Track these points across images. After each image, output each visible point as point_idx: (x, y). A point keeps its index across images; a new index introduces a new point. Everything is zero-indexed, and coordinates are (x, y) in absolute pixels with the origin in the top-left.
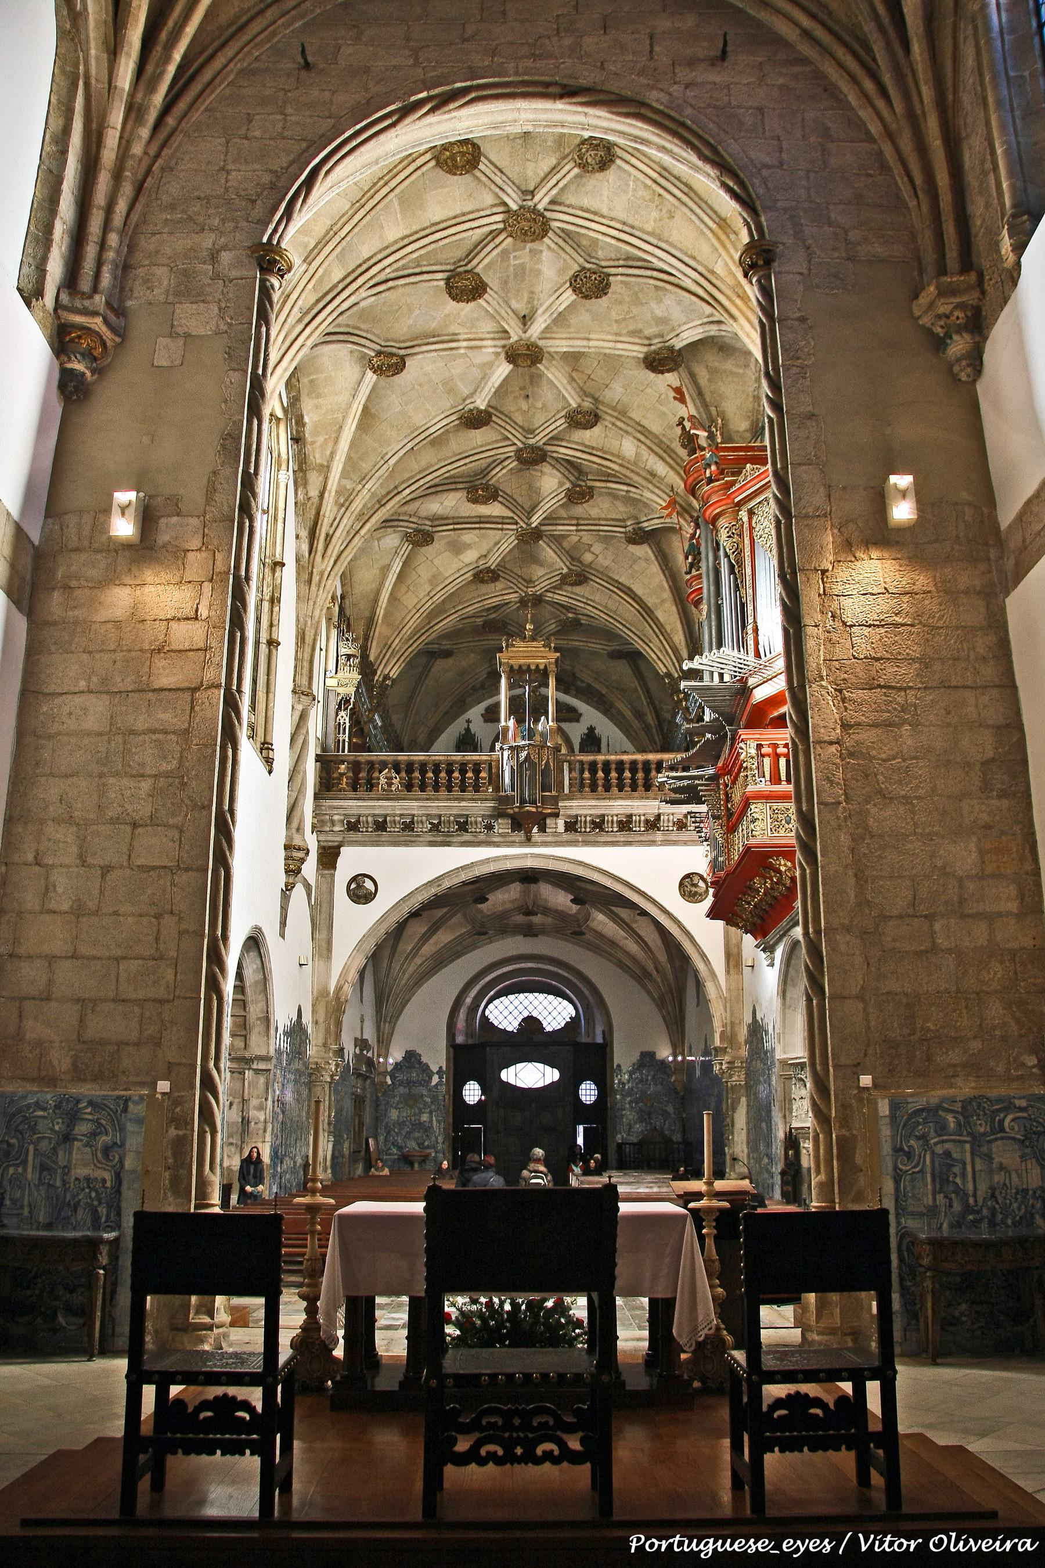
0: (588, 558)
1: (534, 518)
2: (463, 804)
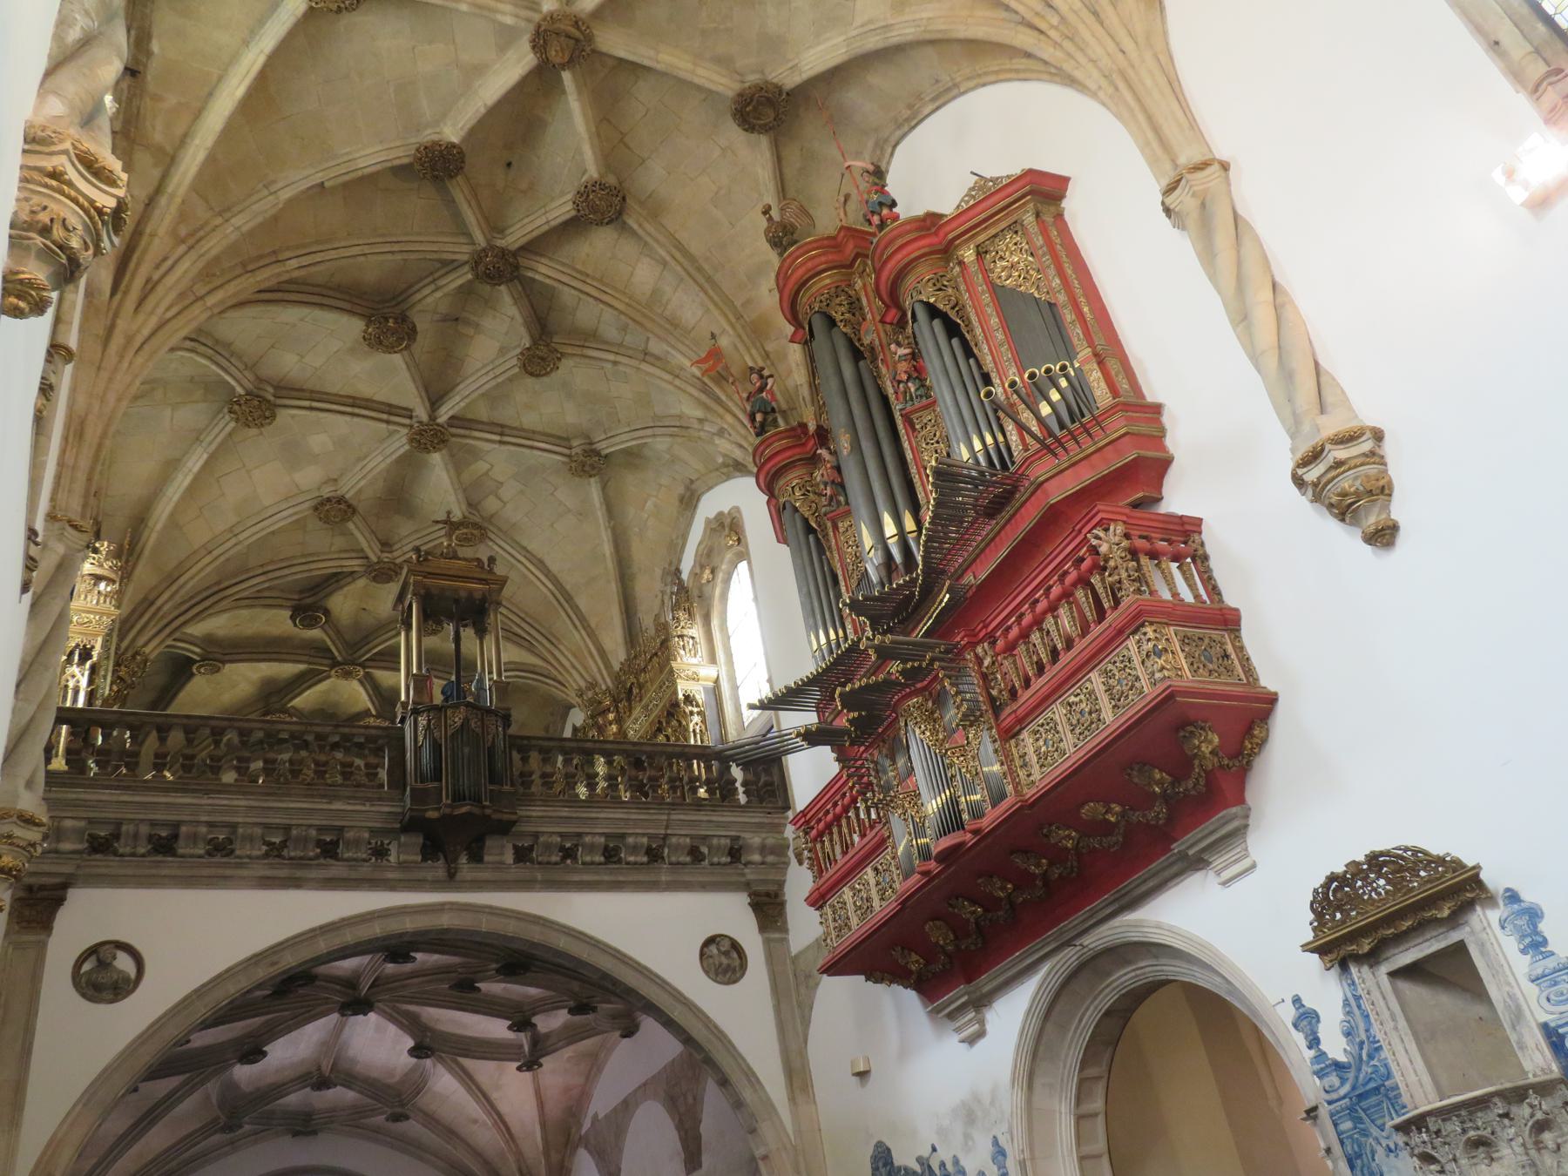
0: (491, 505)
1: (443, 410)
2: (337, 806)
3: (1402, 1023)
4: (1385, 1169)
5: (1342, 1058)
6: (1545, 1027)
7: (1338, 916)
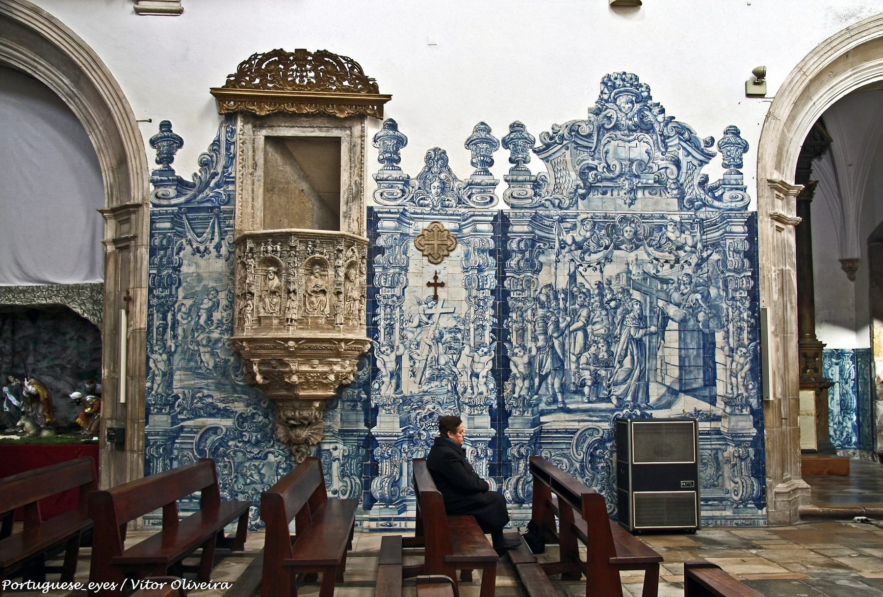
3: (260, 172)
4: (185, 262)
5: (188, 178)
6: (370, 209)
7: (257, 81)
